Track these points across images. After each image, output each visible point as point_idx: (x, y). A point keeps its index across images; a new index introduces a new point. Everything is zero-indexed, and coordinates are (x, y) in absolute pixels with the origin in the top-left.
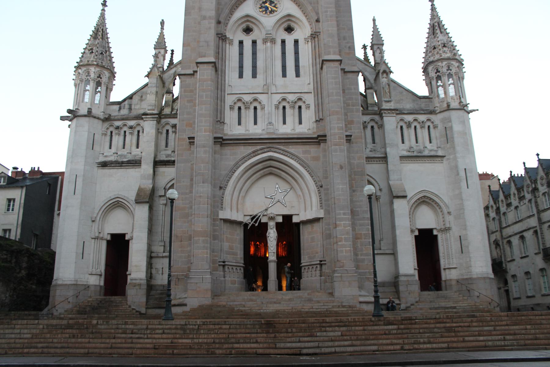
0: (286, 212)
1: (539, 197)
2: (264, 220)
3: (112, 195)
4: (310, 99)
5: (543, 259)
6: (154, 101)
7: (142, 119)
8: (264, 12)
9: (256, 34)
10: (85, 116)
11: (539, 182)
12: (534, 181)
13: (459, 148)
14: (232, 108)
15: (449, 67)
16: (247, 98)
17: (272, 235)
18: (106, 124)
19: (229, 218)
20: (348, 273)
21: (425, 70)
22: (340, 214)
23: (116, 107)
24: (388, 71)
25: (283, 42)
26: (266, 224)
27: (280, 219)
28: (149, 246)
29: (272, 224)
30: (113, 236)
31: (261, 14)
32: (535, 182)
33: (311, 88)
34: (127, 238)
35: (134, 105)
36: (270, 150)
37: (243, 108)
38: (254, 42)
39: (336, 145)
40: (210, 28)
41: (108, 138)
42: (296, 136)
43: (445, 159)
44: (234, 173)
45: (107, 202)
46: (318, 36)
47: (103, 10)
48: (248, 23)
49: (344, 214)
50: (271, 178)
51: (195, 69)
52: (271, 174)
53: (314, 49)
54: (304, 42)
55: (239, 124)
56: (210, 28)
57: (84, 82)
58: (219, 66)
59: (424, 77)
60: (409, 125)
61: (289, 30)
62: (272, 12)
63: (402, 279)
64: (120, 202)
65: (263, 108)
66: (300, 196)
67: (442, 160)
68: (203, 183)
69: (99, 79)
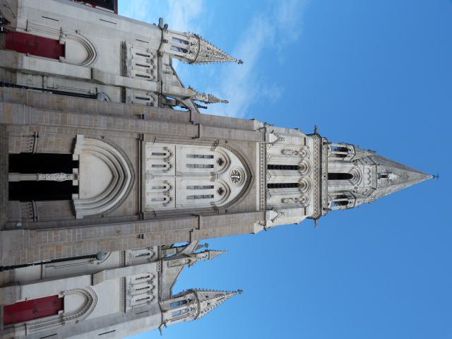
2: (75, 170)
3: (99, 50)
7: (158, 81)
9: (218, 168)
10: (162, 37)
13: (132, 323)
14: (165, 148)
16: (172, 160)
17: (61, 177)
18: (155, 53)
19: (77, 142)
21: (190, 291)
22: (79, 232)
23: (168, 62)
26: (71, 172)
27: (75, 183)
28: (54, 76)
29: (71, 177)
30: (63, 46)
33: (179, 207)
38: (212, 166)
40: (223, 135)
41: (145, 53)
49: (79, 236)
51: (194, 123)
52: (113, 177)
53: (207, 209)
55: (153, 154)
56: (223, 135)
58: (196, 140)
59: (185, 290)
60: (150, 282)
63: (18, 288)
65: (164, 171)
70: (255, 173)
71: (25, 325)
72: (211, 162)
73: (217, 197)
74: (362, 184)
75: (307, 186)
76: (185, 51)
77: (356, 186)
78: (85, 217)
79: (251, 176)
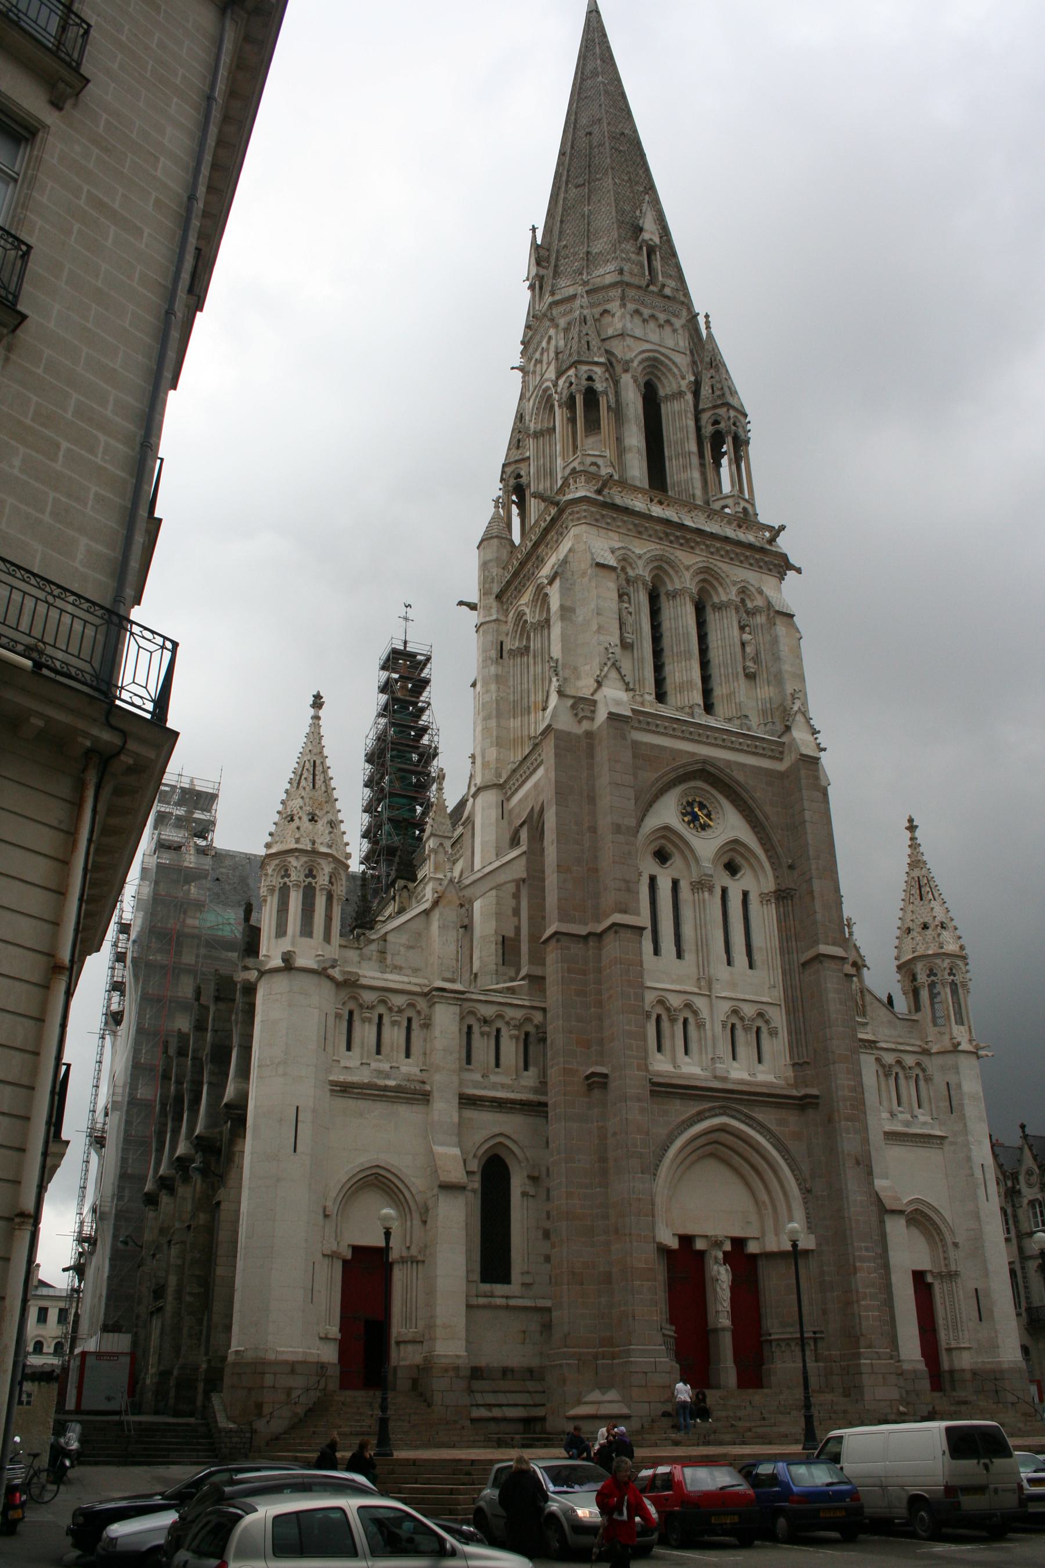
0: (737, 1233)
1: (1021, 1206)
2: (700, 1245)
4: (778, 1018)
5: (1026, 1329)
6: (454, 962)
8: (692, 825)
9: (676, 866)
11: (1022, 1178)
12: (1012, 1174)
15: (951, 969)
16: (675, 1001)
17: (722, 1276)
20: (879, 1359)
24: (860, 962)
25: (724, 891)
31: (686, 826)
32: (1015, 1177)
35: (393, 955)
36: (724, 1111)
37: (665, 1017)
39: (848, 1120)
41: (345, 1024)
42: (765, 1090)
43: (946, 1142)
44: (666, 1151)
45: (355, 1175)
46: (792, 896)
47: (316, 718)
48: (663, 841)
49: (867, 1249)
50: (712, 1165)
52: (712, 1155)
53: (783, 921)
54: (760, 899)
61: (732, 868)
62: (704, 827)
64: (380, 1178)
65: (700, 1026)
66: (764, 1203)
67: (942, 1144)
68: (642, 1173)
69: (310, 879)
70: (705, 761)
71: (949, 1350)
73: (746, 881)
75: (708, 579)
76: (309, 894)
77: (684, 384)
79: (703, 770)
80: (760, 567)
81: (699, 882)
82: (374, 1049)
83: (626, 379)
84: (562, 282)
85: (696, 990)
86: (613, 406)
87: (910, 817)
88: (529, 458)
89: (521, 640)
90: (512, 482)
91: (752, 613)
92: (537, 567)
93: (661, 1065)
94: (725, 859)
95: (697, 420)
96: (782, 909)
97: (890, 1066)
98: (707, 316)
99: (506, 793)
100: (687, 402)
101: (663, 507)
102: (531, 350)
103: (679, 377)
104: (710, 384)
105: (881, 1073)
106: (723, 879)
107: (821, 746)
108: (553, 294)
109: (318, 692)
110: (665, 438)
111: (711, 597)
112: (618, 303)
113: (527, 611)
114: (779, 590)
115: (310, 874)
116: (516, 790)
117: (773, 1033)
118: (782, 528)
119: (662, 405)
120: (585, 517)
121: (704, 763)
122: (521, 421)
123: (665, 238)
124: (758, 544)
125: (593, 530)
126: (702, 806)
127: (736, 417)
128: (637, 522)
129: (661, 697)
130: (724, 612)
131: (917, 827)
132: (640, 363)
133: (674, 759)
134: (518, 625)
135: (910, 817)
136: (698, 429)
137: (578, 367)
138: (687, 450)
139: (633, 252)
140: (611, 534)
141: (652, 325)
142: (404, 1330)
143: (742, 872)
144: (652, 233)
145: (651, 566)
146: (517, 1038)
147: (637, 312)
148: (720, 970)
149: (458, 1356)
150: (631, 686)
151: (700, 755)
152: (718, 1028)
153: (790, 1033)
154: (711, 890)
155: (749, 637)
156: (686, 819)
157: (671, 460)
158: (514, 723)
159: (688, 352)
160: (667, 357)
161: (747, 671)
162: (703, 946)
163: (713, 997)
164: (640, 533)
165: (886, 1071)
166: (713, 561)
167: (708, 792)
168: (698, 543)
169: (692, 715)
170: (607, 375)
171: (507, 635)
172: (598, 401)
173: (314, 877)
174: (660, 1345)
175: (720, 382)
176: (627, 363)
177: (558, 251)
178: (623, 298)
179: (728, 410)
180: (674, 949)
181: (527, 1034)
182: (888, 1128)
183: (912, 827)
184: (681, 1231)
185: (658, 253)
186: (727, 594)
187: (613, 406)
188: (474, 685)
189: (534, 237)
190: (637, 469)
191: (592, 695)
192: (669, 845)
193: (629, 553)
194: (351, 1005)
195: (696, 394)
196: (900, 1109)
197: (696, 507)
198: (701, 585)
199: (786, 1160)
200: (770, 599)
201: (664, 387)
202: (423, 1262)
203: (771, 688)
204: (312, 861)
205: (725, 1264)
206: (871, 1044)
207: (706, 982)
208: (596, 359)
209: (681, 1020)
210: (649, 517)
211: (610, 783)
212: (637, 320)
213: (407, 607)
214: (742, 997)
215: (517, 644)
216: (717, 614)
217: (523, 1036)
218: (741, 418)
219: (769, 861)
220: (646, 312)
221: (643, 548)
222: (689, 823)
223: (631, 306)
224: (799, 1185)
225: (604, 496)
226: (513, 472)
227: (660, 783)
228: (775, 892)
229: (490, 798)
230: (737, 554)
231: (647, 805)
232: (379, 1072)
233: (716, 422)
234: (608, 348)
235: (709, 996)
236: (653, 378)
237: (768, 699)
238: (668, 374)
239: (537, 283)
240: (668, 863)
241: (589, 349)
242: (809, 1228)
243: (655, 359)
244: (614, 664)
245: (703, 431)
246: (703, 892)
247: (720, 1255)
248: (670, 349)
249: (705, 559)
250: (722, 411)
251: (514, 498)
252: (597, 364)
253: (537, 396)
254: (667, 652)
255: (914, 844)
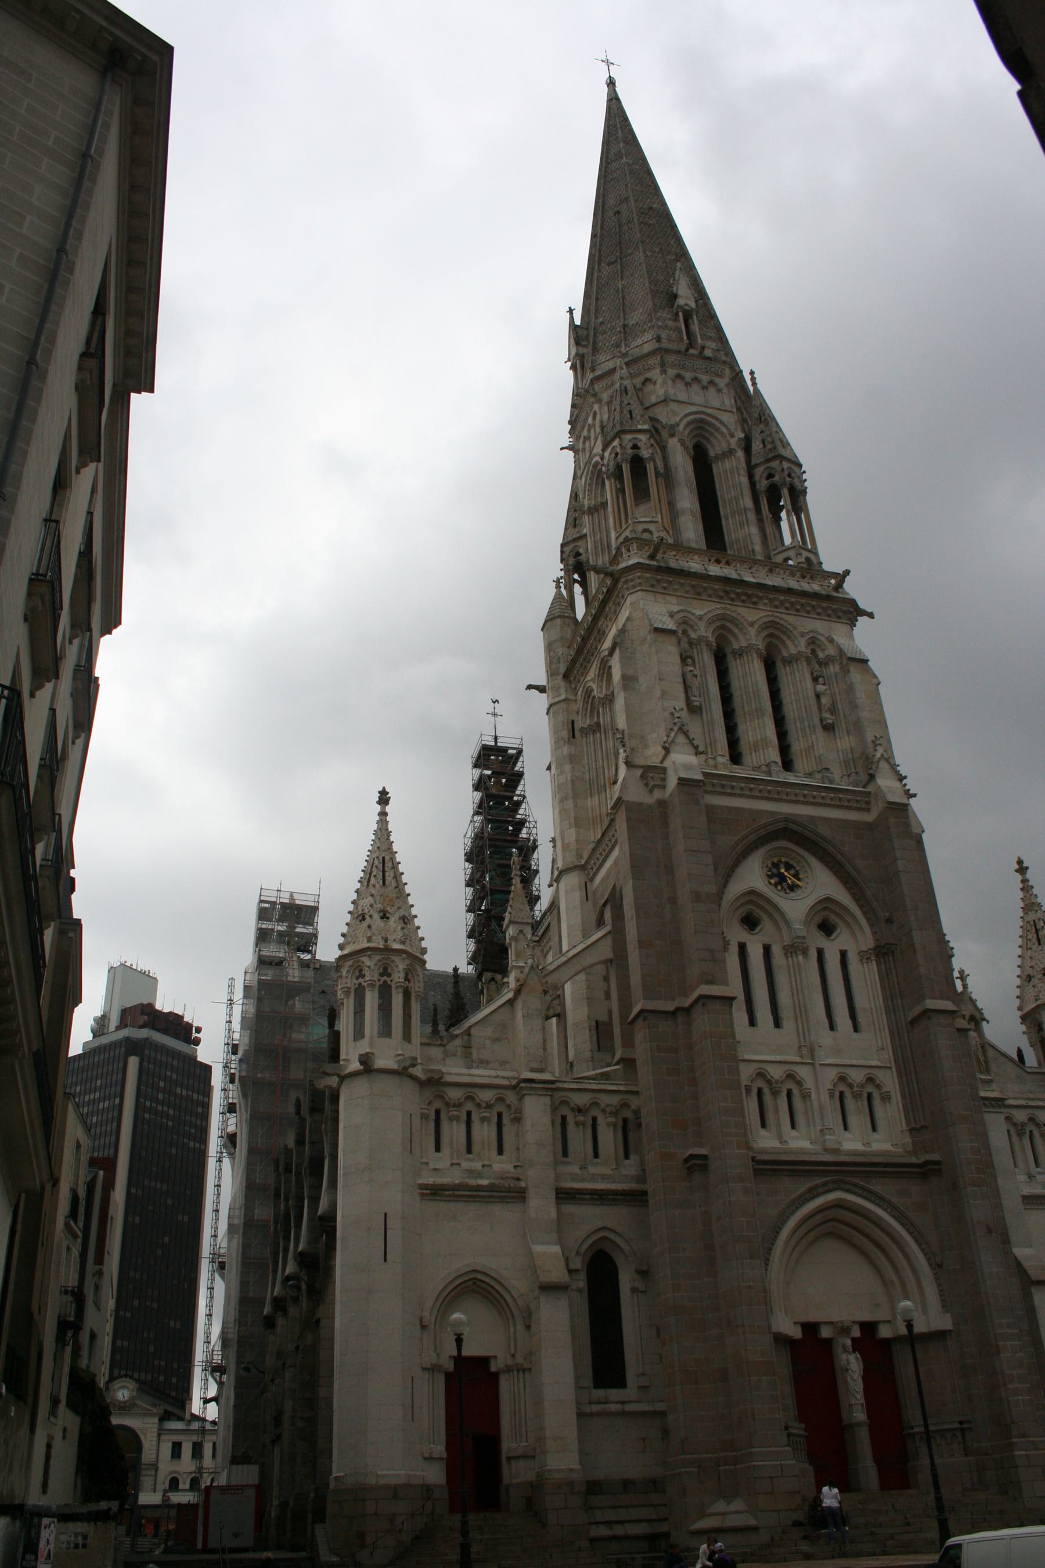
0: (866, 1317)
2: (825, 1333)
3: (461, 1264)
4: (890, 1081)
6: (541, 1051)
8: (779, 887)
9: (767, 931)
14: (748, 1089)
16: (776, 1073)
17: (852, 1365)
24: (978, 1017)
25: (820, 953)
31: (773, 888)
33: (888, 1055)
34: (493, 1368)
36: (838, 1185)
37: (766, 1091)
41: (432, 1125)
42: (881, 1160)
44: (778, 1233)
46: (893, 952)
47: (383, 814)
48: (749, 907)
52: (831, 1234)
53: (885, 978)
57: (377, 988)
61: (827, 929)
62: (793, 888)
64: (478, 1282)
65: (806, 1096)
68: (751, 1258)
70: (787, 819)
72: (755, 954)
73: (842, 940)
74: (725, 417)
75: (775, 633)
76: (385, 992)
77: (733, 442)
78: (945, 1306)
79: (785, 829)
80: (829, 616)
81: (792, 946)
82: (464, 1149)
83: (673, 444)
84: (602, 358)
85: (798, 1059)
86: (662, 471)
87: (1019, 858)
88: (585, 535)
89: (592, 716)
90: (571, 561)
91: (824, 663)
92: (599, 641)
93: (766, 1141)
94: (818, 919)
95: (751, 476)
96: (883, 967)
97: (1023, 1125)
98: (752, 373)
99: (589, 874)
100: (738, 459)
101: (721, 565)
102: (578, 429)
103: (727, 435)
104: (760, 439)
105: (1012, 1132)
106: (819, 940)
107: (911, 792)
108: (593, 370)
109: (384, 788)
110: (719, 498)
111: (780, 651)
112: (658, 370)
113: (594, 686)
114: (851, 637)
115: (385, 972)
116: (599, 869)
117: (886, 1098)
118: (847, 573)
119: (713, 465)
120: (640, 584)
121: (786, 821)
122: (576, 500)
123: (701, 302)
124: (823, 592)
125: (650, 597)
126: (789, 867)
127: (790, 468)
128: (694, 583)
129: (736, 758)
130: (795, 665)
131: (1027, 868)
132: (687, 426)
133: (754, 820)
134: (588, 703)
135: (1019, 858)
136: (753, 484)
137: (623, 436)
138: (742, 506)
139: (670, 319)
140: (669, 598)
141: (696, 387)
142: (514, 1445)
143: (838, 931)
144: (687, 298)
145: (714, 626)
146: (615, 1125)
147: (679, 376)
148: (823, 1037)
149: (571, 1470)
150: (701, 749)
151: (781, 814)
152: (825, 1097)
153: (903, 1096)
154: (805, 952)
155: (824, 687)
156: (773, 881)
157: (727, 518)
158: (592, 802)
159: (735, 410)
160: (713, 417)
161: (824, 723)
162: (801, 1012)
163: (817, 1065)
164: (699, 594)
165: (1018, 1129)
166: (778, 615)
167: (793, 850)
168: (760, 598)
169: (770, 774)
170: (652, 441)
171: (578, 713)
172: (645, 467)
173: (389, 975)
174: (785, 1446)
175: (771, 435)
176: (672, 427)
177: (595, 328)
178: (662, 365)
179: (781, 462)
180: (771, 1017)
181: (625, 1121)
182: (1027, 1191)
183: (1022, 869)
184: (804, 1319)
185: (695, 317)
186: (796, 646)
187: (662, 471)
188: (549, 768)
189: (572, 319)
190: (692, 531)
191: (662, 762)
192: (757, 910)
193: (690, 616)
194: (438, 1104)
195: (747, 449)
196: (1038, 1170)
197: (756, 562)
198: (768, 640)
199: (911, 1234)
200: (842, 646)
201: (713, 447)
202: (530, 1369)
203: (851, 737)
204: (387, 959)
205: (854, 1352)
206: (998, 1103)
207: (809, 1050)
208: (639, 427)
209: (785, 1092)
210: (707, 577)
211: (685, 850)
212: (680, 385)
213: (494, 702)
214: (849, 1062)
215: (588, 722)
216: (787, 668)
217: (620, 1123)
218: (796, 469)
219: (865, 916)
220: (688, 376)
221: (703, 609)
222: (776, 885)
223: (671, 372)
224: (928, 1260)
225: (657, 561)
226: (571, 551)
227: (740, 846)
228: (874, 949)
229: (572, 880)
230: (802, 605)
231: (727, 871)
232: (471, 1172)
233: (770, 476)
234: (652, 416)
235: (813, 1064)
236: (701, 440)
237: (849, 750)
238: (716, 434)
239: (578, 362)
240: (758, 928)
241: (631, 418)
242: (943, 1306)
243: (702, 421)
244: (680, 729)
245: (758, 486)
246: (797, 956)
247: (849, 1342)
248: (715, 408)
249: (770, 613)
250: (775, 464)
251: (576, 576)
252: (640, 431)
253: (587, 473)
254: (738, 712)
255: (1026, 887)
